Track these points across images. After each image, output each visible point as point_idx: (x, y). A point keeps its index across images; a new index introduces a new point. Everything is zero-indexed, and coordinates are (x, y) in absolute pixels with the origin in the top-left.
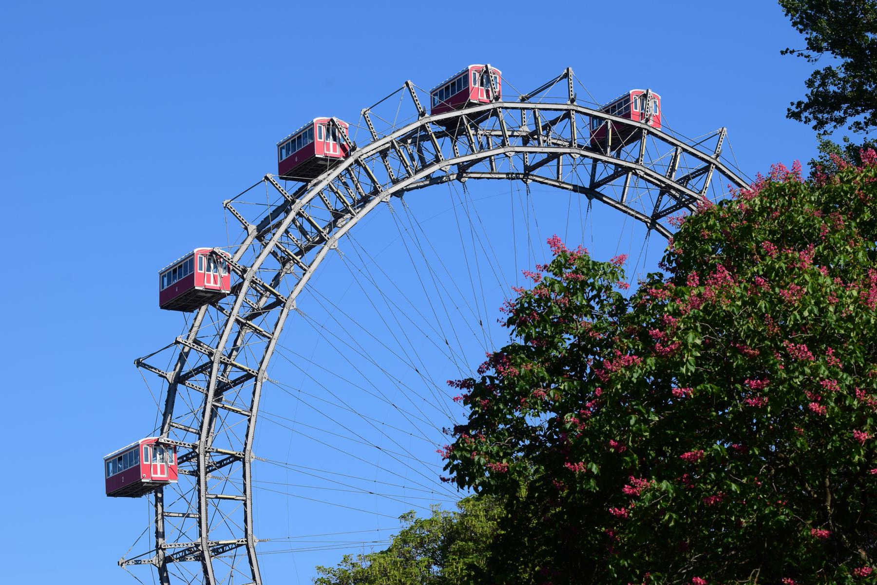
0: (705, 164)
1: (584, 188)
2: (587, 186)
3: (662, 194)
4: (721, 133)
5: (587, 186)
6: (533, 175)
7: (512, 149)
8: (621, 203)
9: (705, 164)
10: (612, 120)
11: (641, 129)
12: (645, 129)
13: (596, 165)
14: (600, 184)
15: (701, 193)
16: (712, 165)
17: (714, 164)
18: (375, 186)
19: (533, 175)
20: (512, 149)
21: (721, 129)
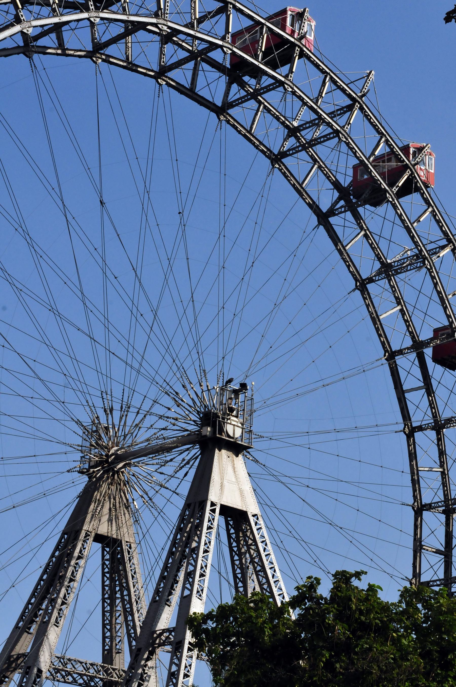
0: (349, 102)
1: (215, 105)
2: (219, 103)
3: (289, 136)
4: (368, 76)
5: (219, 103)
6: (166, 77)
7: (165, 22)
8: (250, 132)
9: (349, 102)
10: (268, 27)
11: (293, 45)
12: (299, 47)
13: (230, 87)
14: (232, 105)
15: (344, 126)
16: (357, 104)
17: (359, 103)
18: (17, 14)
19: (166, 77)
20: (165, 22)
21: (368, 72)
